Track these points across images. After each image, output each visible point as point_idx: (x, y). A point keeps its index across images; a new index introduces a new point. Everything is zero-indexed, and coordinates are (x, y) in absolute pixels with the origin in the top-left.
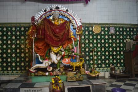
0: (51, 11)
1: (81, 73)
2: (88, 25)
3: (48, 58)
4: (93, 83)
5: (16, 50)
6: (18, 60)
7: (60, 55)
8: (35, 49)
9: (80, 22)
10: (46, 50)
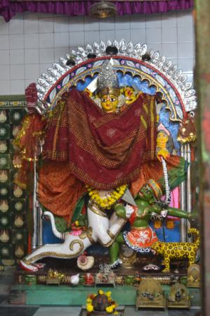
0: (92, 63)
3: (79, 226)
7: (120, 217)
8: (42, 193)
10: (75, 199)
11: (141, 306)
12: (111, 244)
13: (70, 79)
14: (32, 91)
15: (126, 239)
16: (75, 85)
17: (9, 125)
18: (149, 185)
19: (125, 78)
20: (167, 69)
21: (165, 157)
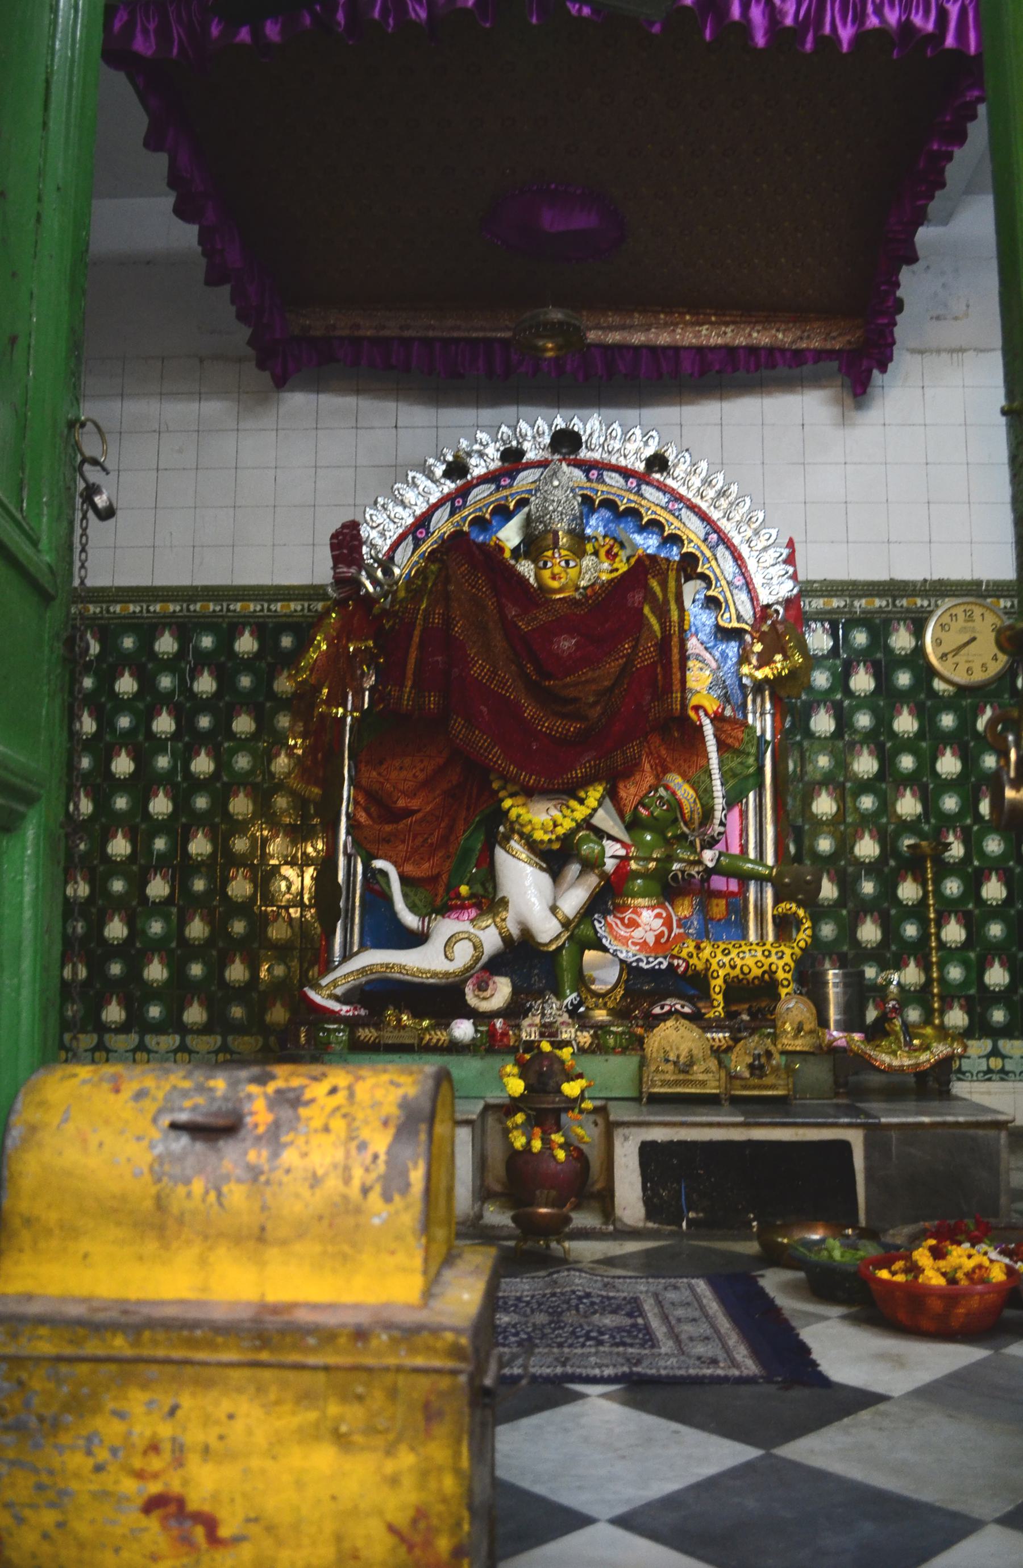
2: (878, 603)
3: (472, 895)
6: (197, 929)
8: (362, 817)
9: (781, 568)
11: (656, 1090)
12: (560, 942)
13: (452, 514)
15: (601, 932)
16: (466, 528)
17: (263, 665)
18: (667, 788)
20: (711, 493)
21: (710, 711)
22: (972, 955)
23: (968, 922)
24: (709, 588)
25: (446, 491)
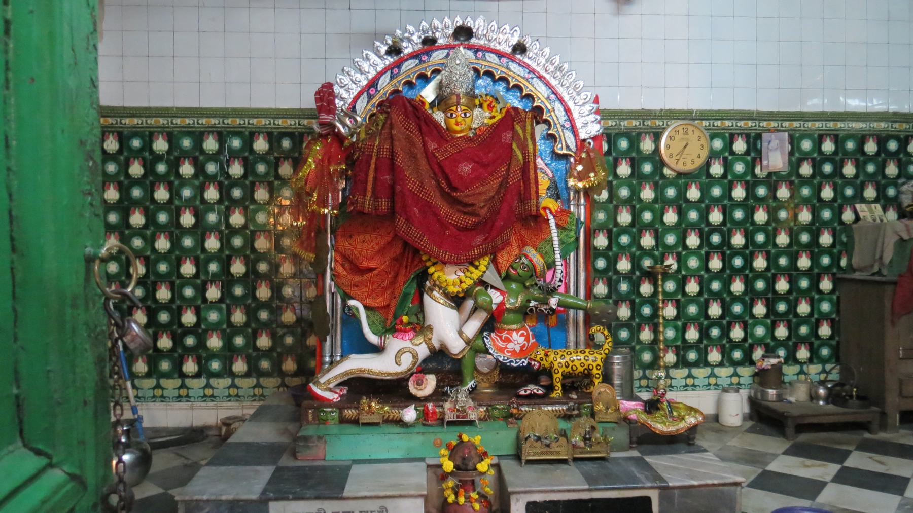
0: (428, 53)
1: (593, 415)
2: (635, 123)
3: (409, 323)
4: (665, 475)
5: (226, 264)
6: (238, 317)
8: (340, 270)
9: (592, 117)
10: (401, 279)
11: (531, 458)
12: (464, 353)
13: (392, 78)
14: (326, 95)
16: (400, 88)
17: (272, 158)
18: (527, 257)
19: (480, 81)
20: (551, 68)
22: (679, 323)
23: (678, 305)
24: (549, 129)
25: (387, 63)
